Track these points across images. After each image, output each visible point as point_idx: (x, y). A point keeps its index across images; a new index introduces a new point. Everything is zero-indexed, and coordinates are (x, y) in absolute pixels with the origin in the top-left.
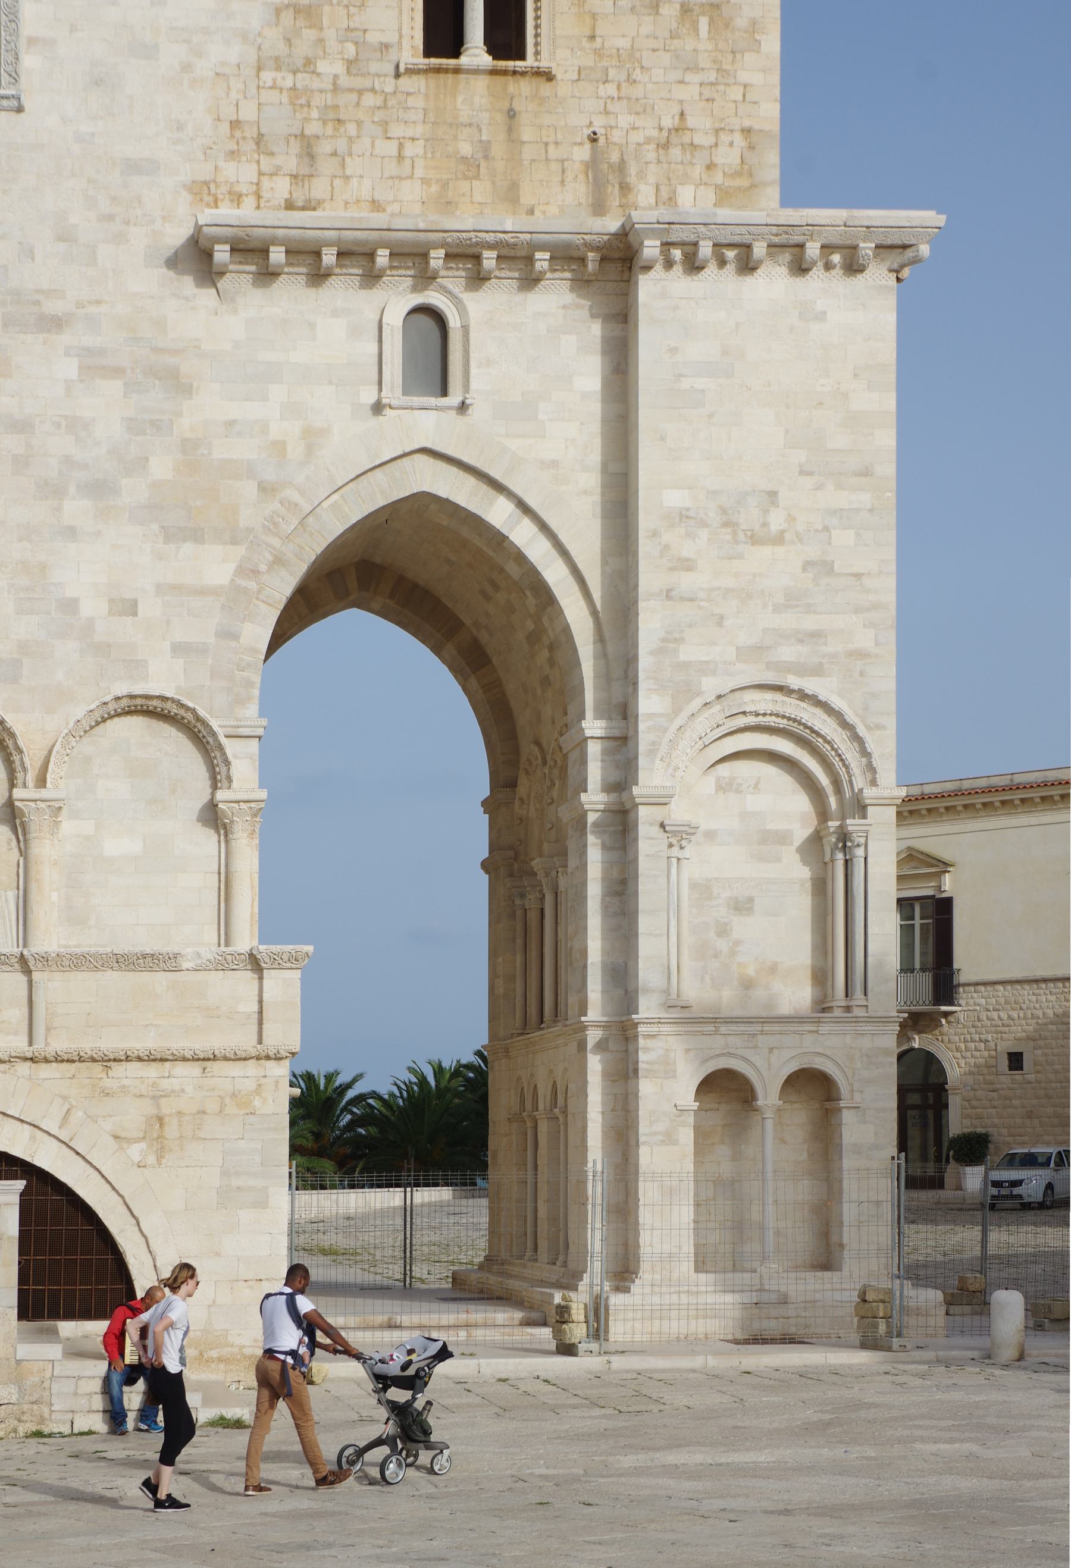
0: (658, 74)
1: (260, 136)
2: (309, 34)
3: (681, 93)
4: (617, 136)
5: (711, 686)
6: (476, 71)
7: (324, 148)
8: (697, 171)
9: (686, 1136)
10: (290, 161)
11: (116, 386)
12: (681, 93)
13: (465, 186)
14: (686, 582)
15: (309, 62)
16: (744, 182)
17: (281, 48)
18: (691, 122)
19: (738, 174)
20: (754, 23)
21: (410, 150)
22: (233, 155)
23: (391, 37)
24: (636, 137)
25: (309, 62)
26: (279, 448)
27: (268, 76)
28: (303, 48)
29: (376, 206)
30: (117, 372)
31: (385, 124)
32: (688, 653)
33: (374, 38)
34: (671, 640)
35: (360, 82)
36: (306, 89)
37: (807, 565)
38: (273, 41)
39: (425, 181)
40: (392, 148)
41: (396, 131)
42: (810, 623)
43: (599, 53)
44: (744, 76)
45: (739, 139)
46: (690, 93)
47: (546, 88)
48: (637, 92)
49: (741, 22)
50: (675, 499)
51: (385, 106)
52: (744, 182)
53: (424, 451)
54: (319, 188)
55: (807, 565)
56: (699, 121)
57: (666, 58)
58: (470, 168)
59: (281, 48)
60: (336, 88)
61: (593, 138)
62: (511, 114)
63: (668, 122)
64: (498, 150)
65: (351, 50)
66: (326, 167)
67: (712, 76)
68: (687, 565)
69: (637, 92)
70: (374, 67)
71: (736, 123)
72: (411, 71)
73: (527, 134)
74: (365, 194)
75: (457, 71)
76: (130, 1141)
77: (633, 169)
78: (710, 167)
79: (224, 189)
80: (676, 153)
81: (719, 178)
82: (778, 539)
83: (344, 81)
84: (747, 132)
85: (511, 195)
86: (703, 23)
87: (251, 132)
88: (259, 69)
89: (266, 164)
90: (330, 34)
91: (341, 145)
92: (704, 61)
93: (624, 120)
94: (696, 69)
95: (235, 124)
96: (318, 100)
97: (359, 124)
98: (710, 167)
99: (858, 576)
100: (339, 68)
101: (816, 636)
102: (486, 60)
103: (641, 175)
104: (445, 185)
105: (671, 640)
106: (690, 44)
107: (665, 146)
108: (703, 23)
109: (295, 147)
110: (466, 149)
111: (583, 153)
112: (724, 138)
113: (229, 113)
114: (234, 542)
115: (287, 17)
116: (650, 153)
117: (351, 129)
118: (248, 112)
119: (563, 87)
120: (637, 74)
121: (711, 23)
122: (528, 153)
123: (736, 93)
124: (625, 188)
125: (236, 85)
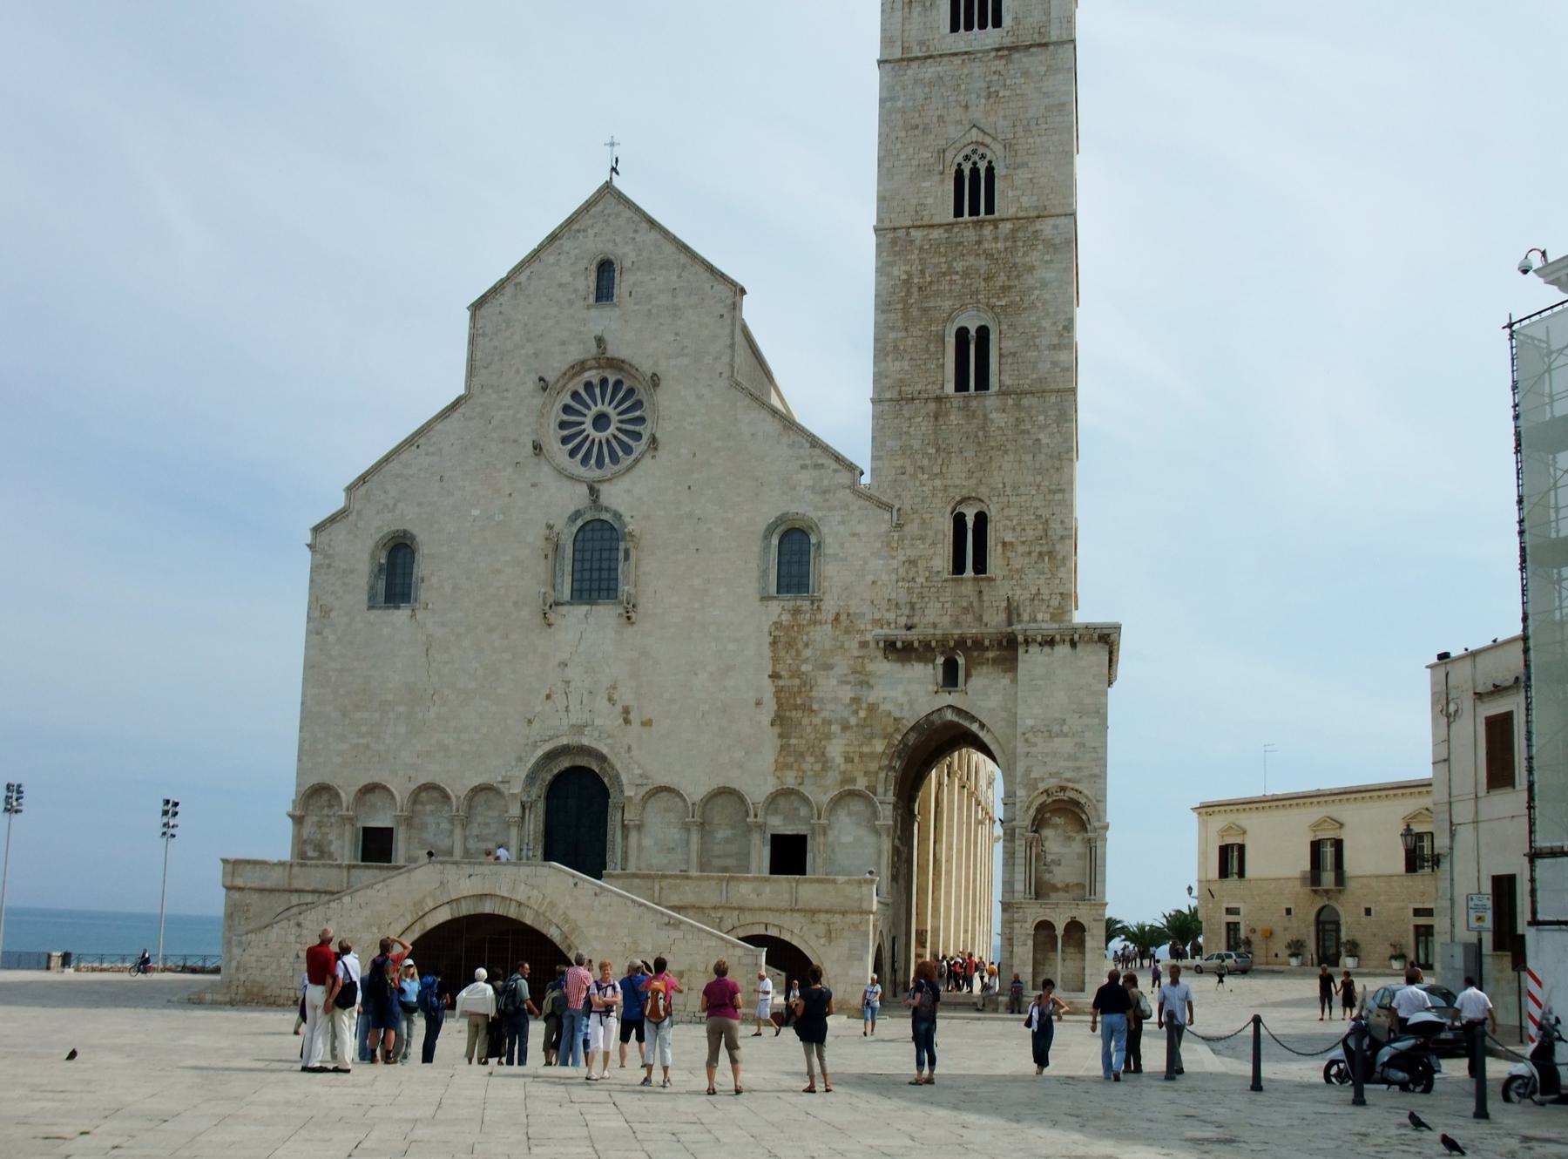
0: (1030, 576)
1: (897, 604)
2: (914, 569)
3: (1038, 582)
4: (1016, 598)
5: (1042, 786)
6: (967, 580)
7: (918, 606)
8: (1044, 608)
9: (1030, 943)
10: (907, 611)
11: (849, 687)
12: (1038, 582)
13: (964, 617)
14: (1034, 750)
15: (913, 578)
16: (1060, 611)
17: (904, 574)
18: (1041, 592)
19: (1058, 609)
20: (1064, 557)
21: (946, 605)
22: (888, 610)
23: (940, 569)
24: (1022, 598)
25: (913, 578)
26: (901, 706)
27: (900, 584)
28: (911, 574)
29: (935, 626)
30: (848, 683)
31: (938, 598)
32: (1033, 776)
33: (935, 569)
34: (1028, 771)
35: (929, 584)
36: (913, 588)
37: (1076, 744)
38: (902, 571)
39: (951, 616)
40: (940, 605)
41: (941, 599)
42: (1078, 764)
43: (1010, 570)
44: (1060, 575)
45: (1059, 597)
46: (1042, 582)
47: (992, 583)
48: (1023, 582)
49: (1059, 557)
50: (1030, 722)
51: (938, 592)
52: (1060, 611)
53: (949, 706)
54: (916, 620)
55: (1076, 744)
56: (1045, 592)
57: (1034, 571)
58: (966, 610)
59: (904, 574)
60: (922, 587)
61: (1008, 599)
62: (981, 592)
63: (1033, 592)
64: (975, 604)
65: (927, 574)
66: (919, 612)
67: (1049, 576)
68: (1035, 745)
69: (1023, 582)
70: (935, 579)
71: (1057, 591)
72: (946, 581)
73: (985, 598)
74: (931, 620)
75: (962, 579)
76: (821, 937)
77: (1021, 609)
78: (1048, 606)
79: (884, 622)
80: (1036, 602)
81: (1051, 610)
82: (1066, 735)
83: (925, 584)
84: (1061, 594)
85: (980, 619)
86: (1046, 559)
87: (894, 602)
88: (897, 581)
89: (899, 612)
90: (921, 569)
91: (923, 605)
92: (1046, 571)
93: (1019, 592)
94: (1043, 573)
95: (889, 600)
96: (916, 591)
97: (929, 597)
98: (1048, 606)
99: (1094, 748)
100: (923, 580)
101: (1079, 768)
102: (973, 574)
103: (1024, 610)
104: (957, 616)
105: (1028, 771)
106: (1042, 565)
107: (1033, 599)
108: (1046, 559)
109: (908, 606)
110: (965, 604)
111: (1005, 604)
112: (1054, 596)
113: (887, 597)
114: (885, 738)
115: (907, 564)
116: (1027, 603)
117: (927, 599)
118: (893, 596)
119: (998, 583)
120: (1023, 576)
121: (1049, 558)
122: (985, 604)
123: (1058, 581)
124: (1019, 615)
125: (890, 587)
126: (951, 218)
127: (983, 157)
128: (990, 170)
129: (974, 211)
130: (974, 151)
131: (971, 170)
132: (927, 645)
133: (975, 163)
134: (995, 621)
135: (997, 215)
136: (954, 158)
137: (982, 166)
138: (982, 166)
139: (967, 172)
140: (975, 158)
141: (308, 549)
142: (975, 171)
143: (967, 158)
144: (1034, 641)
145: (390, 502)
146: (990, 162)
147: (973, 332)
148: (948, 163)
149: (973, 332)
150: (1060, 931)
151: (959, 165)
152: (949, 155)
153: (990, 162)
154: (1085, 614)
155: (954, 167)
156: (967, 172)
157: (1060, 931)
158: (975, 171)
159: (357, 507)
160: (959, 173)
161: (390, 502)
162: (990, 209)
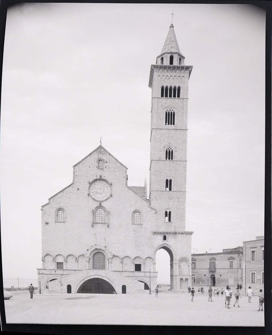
126: (165, 160)
127: (171, 149)
128: (172, 151)
129: (169, 159)
130: (169, 148)
131: (169, 151)
132: (161, 233)
133: (169, 150)
134: (173, 230)
135: (173, 160)
136: (166, 148)
137: (171, 150)
138: (171, 150)
139: (168, 151)
140: (169, 149)
141: (41, 210)
142: (169, 151)
143: (168, 149)
144: (180, 233)
145: (58, 202)
146: (172, 150)
147: (169, 180)
148: (165, 149)
149: (169, 180)
150: (184, 280)
151: (167, 150)
152: (165, 148)
153: (172, 150)
154: (187, 230)
155: (166, 150)
156: (168, 151)
157: (184, 280)
158: (169, 151)
159: (51, 203)
160: (167, 151)
161: (58, 202)
162: (172, 159)
